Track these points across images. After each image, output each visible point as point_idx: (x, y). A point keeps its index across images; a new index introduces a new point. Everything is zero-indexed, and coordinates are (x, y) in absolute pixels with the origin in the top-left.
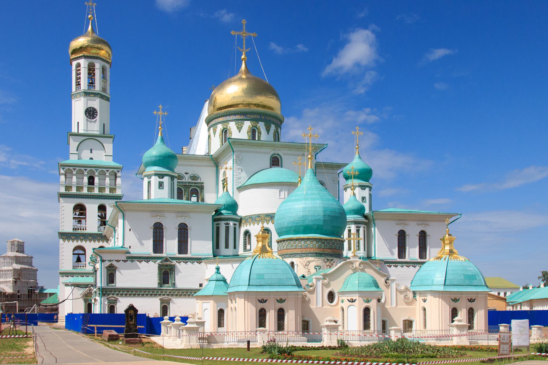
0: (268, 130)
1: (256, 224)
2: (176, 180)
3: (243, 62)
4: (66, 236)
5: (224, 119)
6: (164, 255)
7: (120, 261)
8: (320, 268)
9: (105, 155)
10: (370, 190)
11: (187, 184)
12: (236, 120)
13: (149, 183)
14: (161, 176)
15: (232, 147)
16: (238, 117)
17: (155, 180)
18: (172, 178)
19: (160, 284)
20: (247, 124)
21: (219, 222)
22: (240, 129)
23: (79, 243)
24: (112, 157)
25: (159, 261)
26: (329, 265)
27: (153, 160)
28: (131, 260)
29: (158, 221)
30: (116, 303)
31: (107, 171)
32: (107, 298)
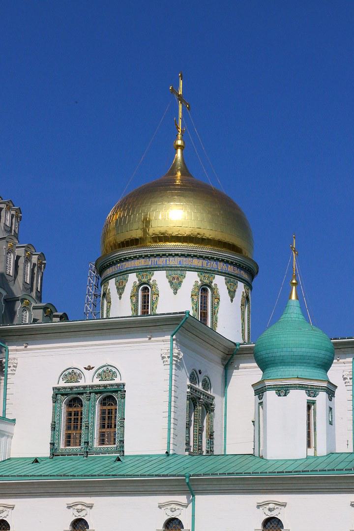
5: (205, 265)
12: (228, 274)
16: (230, 269)
27: (321, 356)
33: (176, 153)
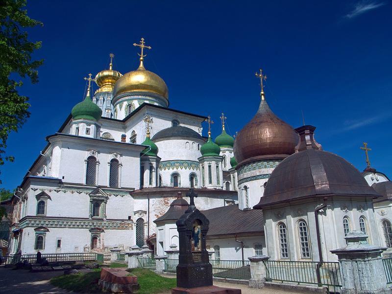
1: (167, 169)
3: (142, 62)
16: (140, 97)
21: (143, 162)
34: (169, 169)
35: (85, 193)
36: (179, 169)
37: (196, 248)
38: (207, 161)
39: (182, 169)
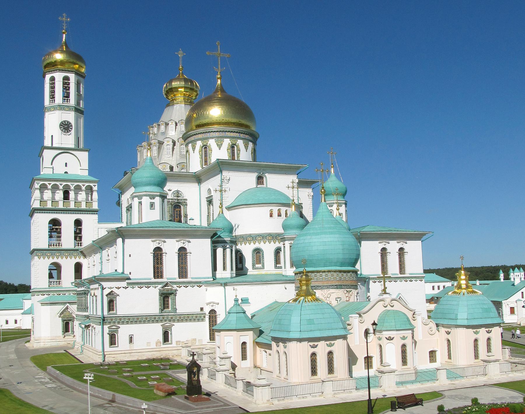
0: (246, 147)
2: (166, 200)
4: (41, 253)
5: (204, 136)
6: (164, 280)
7: (121, 287)
8: (340, 299)
9: (80, 169)
10: (346, 207)
11: (171, 201)
13: (140, 203)
14: (153, 197)
15: (220, 167)
17: (146, 201)
18: (163, 197)
19: (162, 310)
20: (227, 142)
21: (216, 245)
22: (220, 146)
23: (55, 260)
24: (88, 170)
25: (160, 286)
26: (348, 296)
28: (132, 286)
29: (159, 246)
30: (118, 331)
31: (84, 185)
32: (108, 327)
33: (218, 81)
34: (250, 244)
35: (153, 287)
36: (262, 243)
37: (194, 378)
38: (289, 240)
39: (265, 243)
